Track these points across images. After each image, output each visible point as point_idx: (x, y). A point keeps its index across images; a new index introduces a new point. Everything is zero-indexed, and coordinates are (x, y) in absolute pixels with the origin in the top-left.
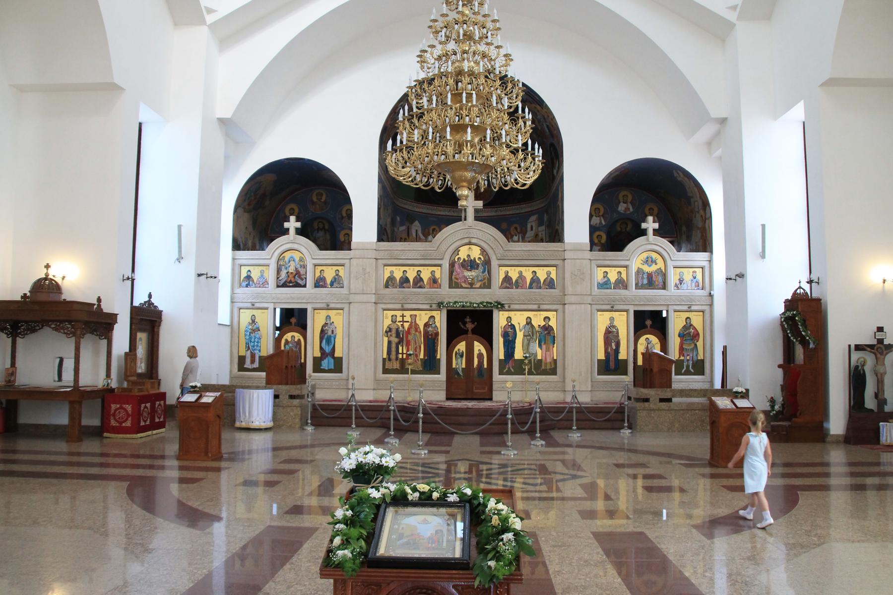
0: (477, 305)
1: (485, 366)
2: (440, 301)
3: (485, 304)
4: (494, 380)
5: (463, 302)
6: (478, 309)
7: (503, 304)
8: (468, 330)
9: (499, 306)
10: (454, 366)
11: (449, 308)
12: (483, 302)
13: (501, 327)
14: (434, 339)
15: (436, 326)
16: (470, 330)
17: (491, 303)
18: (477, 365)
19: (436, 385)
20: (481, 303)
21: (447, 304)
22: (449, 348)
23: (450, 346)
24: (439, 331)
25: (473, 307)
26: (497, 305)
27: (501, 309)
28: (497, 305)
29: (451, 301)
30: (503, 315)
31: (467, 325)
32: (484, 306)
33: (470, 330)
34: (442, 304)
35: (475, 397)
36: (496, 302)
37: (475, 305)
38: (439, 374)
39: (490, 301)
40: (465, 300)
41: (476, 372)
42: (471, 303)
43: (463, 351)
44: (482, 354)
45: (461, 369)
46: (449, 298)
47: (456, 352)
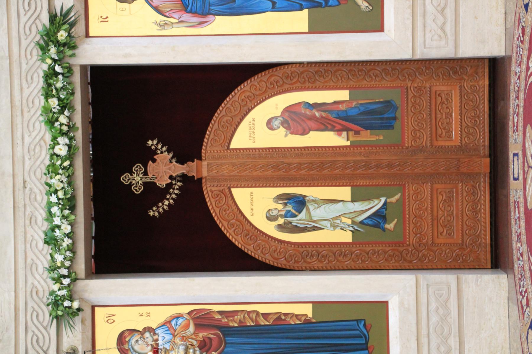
0: (63, 140)
1: (343, 95)
2: (47, 311)
3: (54, 103)
4: (407, 55)
5: (50, 205)
6: (79, 135)
7: (53, 18)
8: (184, 178)
9: (62, 35)
10: (347, 237)
11: (81, 267)
12: (47, 110)
13: (162, 26)
14: (227, 331)
15: (167, 324)
16: (179, 169)
17: (51, 74)
18: (339, 132)
19: (434, 319)
20: (51, 122)
21: (58, 280)
22: (268, 259)
23: (258, 255)
24: (187, 309)
25: (71, 156)
26: (57, 44)
27: (79, 29)
28: (57, 44)
29: (44, 262)
30: (105, 20)
31: (162, 183)
32: (64, 106)
33: (179, 169)
34: (56, 303)
35: (484, 140)
36: (44, 49)
37: (62, 150)
38: (385, 303)
39: (39, 82)
40: (42, 199)
41: (367, 136)
42: (52, 170)
43: (280, 197)
44: (289, 110)
45: (359, 206)
46: (31, 268)
47: (281, 228)
